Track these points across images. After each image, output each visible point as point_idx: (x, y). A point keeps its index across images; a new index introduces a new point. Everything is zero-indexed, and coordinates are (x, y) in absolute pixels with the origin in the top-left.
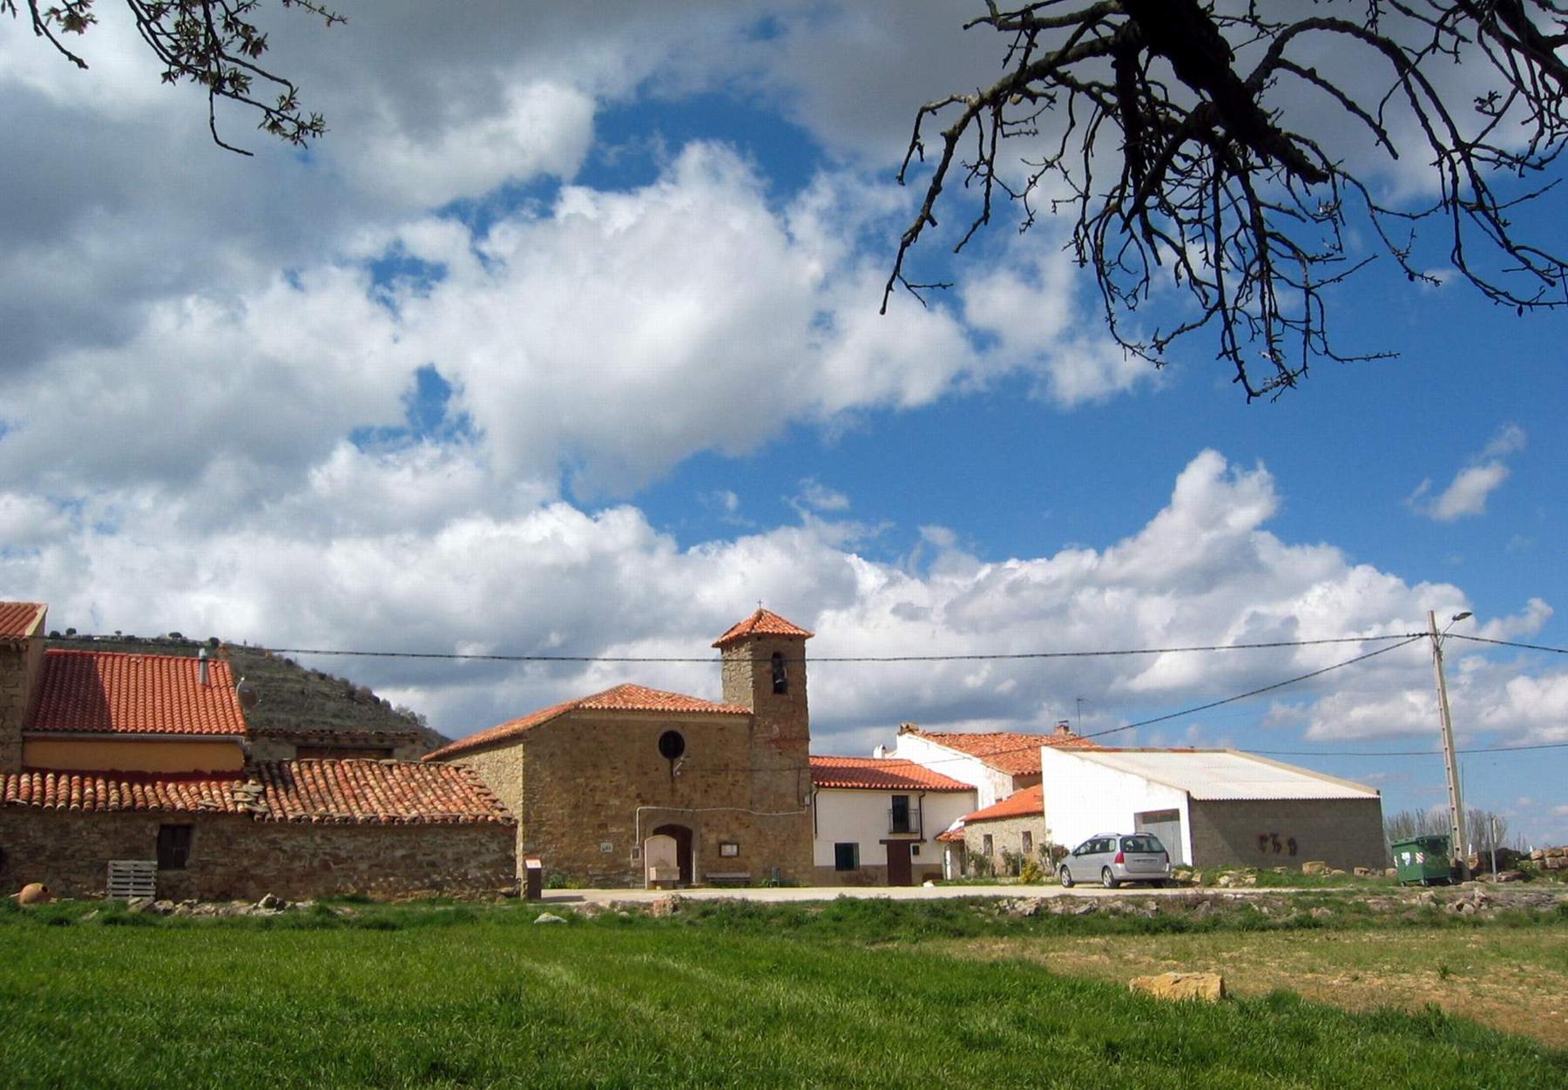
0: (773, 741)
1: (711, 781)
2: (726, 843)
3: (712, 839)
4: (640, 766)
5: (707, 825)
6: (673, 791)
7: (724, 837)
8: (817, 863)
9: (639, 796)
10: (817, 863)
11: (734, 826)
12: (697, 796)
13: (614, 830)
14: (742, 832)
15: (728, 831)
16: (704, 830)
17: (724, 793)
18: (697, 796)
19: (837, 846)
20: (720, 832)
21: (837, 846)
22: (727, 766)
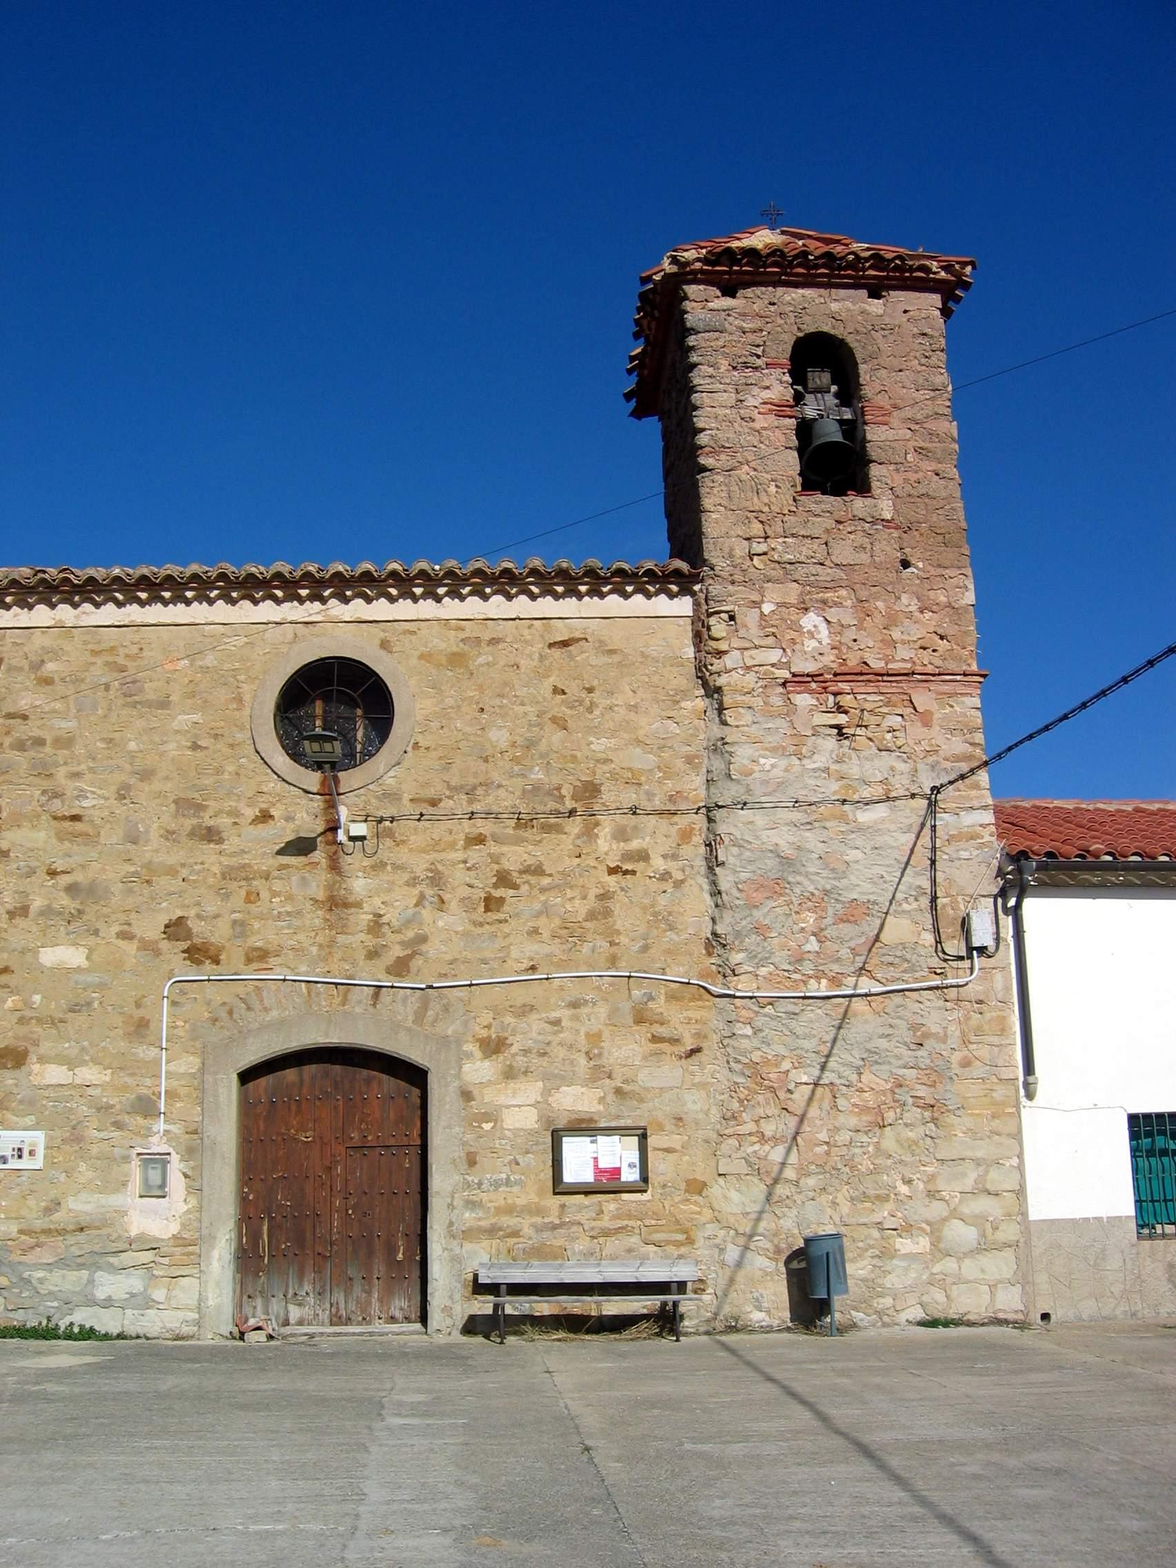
0: (800, 680)
1: (514, 857)
2: (585, 1128)
3: (520, 1110)
4: (186, 805)
5: (493, 1047)
6: (336, 903)
7: (576, 1099)
8: (1045, 1203)
9: (176, 929)
10: (1037, 1211)
11: (627, 1050)
12: (447, 928)
13: (55, 1074)
14: (662, 1074)
15: (599, 1073)
16: (479, 1070)
17: (580, 908)
18: (447, 928)
19: (1133, 1119)
20: (554, 1081)
21: (1133, 1119)
22: (590, 790)
